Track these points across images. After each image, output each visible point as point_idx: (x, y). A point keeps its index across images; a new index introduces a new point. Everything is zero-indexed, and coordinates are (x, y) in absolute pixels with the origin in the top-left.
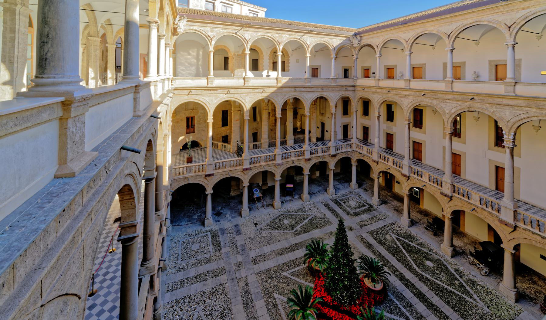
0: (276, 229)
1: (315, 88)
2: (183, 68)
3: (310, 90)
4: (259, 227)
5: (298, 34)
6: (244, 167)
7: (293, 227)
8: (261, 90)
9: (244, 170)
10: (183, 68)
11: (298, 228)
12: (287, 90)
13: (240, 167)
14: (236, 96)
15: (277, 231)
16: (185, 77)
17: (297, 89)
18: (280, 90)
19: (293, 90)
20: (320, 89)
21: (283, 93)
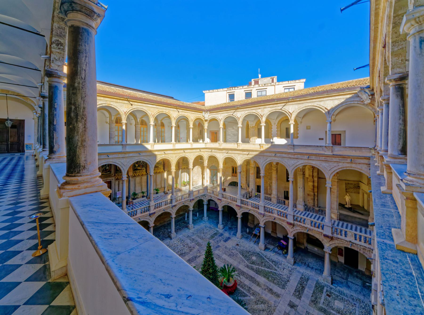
0: (243, 255)
1: (299, 156)
2: (230, 137)
3: (293, 157)
4: (237, 247)
5: (279, 105)
7: (253, 263)
8: (247, 153)
10: (230, 137)
11: (255, 267)
12: (268, 154)
14: (232, 155)
15: (241, 256)
16: (230, 142)
18: (262, 154)
20: (306, 157)
21: (265, 157)
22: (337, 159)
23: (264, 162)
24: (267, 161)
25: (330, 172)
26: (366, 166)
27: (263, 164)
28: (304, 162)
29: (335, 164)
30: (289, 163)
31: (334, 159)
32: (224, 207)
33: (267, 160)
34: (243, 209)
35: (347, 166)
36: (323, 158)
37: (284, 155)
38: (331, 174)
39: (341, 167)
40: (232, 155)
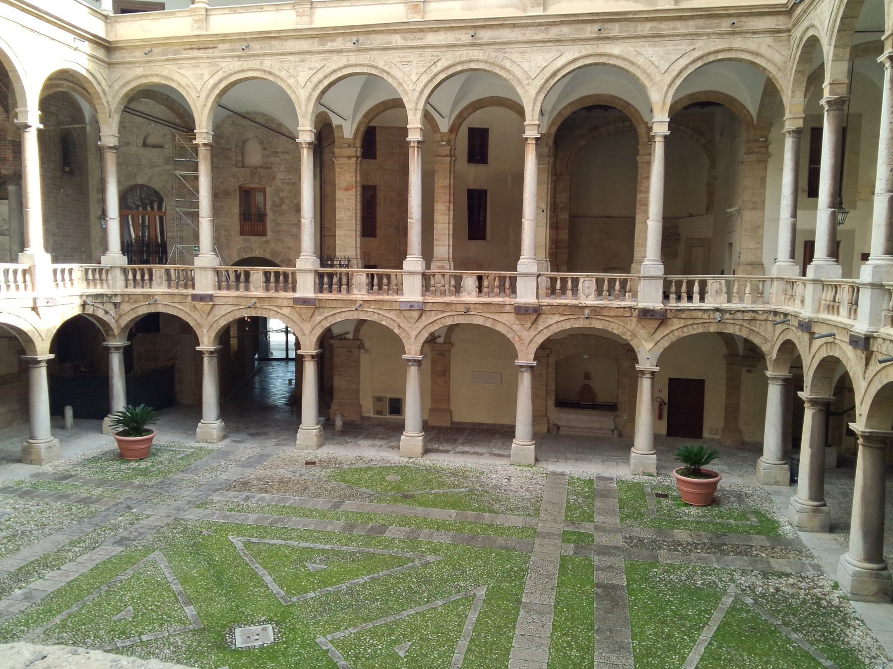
3: (541, 36)
6: (298, 295)
9: (297, 301)
13: (290, 294)
14: (267, 63)
17: (485, 35)
19: (465, 37)
20: (590, 31)
21: (428, 53)
22: (690, 27)
23: (425, 79)
24: (435, 70)
25: (668, 78)
26: (769, 39)
27: (419, 89)
28: (584, 53)
29: (685, 46)
30: (525, 66)
31: (682, 27)
32: (223, 336)
33: (440, 66)
34: (327, 313)
35: (719, 47)
36: (646, 28)
37: (507, 34)
38: (669, 86)
39: (701, 53)
40: (267, 63)
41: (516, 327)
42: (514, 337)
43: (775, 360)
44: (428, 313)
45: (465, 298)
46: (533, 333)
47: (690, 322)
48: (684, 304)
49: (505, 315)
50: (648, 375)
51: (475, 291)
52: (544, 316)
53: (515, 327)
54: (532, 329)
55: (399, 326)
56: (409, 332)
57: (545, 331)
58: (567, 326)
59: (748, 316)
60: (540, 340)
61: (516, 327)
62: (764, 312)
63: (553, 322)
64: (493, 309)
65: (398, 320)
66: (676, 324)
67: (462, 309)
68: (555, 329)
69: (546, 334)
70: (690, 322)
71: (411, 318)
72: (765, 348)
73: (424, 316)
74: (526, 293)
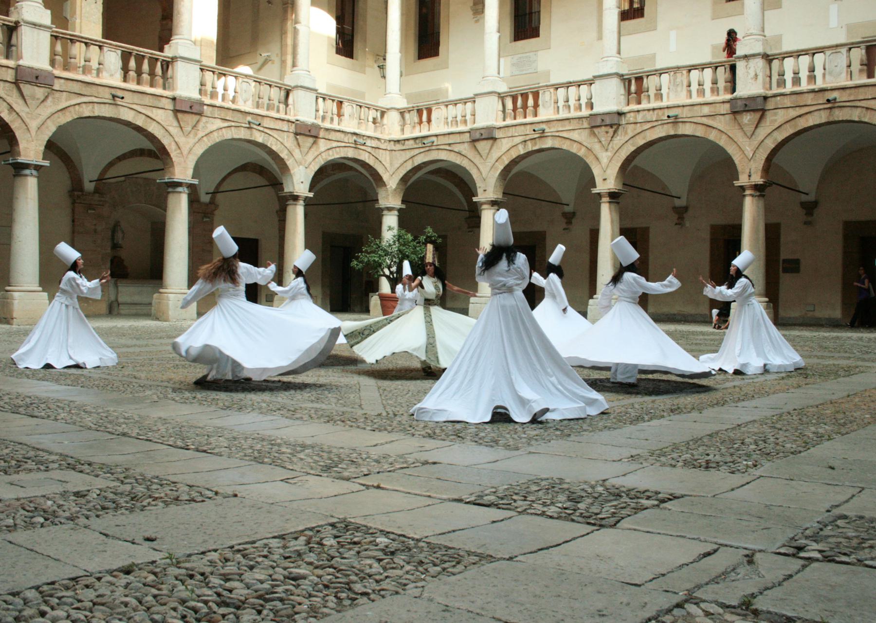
41: (174, 130)
42: (170, 144)
43: (395, 190)
44: (57, 95)
45: (105, 79)
46: (192, 140)
47: (335, 144)
48: (327, 125)
49: (160, 111)
50: (301, 202)
51: (119, 74)
52: (204, 119)
53: (171, 129)
54: (191, 135)
55: (11, 108)
56: (27, 120)
57: (205, 139)
58: (229, 134)
59: (374, 143)
60: (200, 150)
61: (174, 130)
62: (385, 141)
63: (215, 128)
64: (147, 100)
65: (9, 99)
66: (322, 145)
67: (106, 95)
68: (216, 138)
69: (207, 143)
70: (335, 144)
71: (33, 97)
72: (385, 177)
73: (50, 99)
74: (186, 83)
